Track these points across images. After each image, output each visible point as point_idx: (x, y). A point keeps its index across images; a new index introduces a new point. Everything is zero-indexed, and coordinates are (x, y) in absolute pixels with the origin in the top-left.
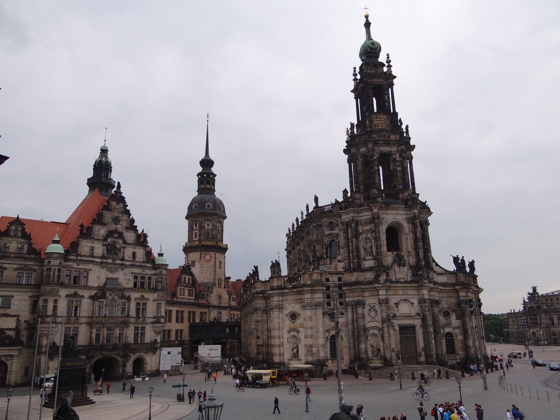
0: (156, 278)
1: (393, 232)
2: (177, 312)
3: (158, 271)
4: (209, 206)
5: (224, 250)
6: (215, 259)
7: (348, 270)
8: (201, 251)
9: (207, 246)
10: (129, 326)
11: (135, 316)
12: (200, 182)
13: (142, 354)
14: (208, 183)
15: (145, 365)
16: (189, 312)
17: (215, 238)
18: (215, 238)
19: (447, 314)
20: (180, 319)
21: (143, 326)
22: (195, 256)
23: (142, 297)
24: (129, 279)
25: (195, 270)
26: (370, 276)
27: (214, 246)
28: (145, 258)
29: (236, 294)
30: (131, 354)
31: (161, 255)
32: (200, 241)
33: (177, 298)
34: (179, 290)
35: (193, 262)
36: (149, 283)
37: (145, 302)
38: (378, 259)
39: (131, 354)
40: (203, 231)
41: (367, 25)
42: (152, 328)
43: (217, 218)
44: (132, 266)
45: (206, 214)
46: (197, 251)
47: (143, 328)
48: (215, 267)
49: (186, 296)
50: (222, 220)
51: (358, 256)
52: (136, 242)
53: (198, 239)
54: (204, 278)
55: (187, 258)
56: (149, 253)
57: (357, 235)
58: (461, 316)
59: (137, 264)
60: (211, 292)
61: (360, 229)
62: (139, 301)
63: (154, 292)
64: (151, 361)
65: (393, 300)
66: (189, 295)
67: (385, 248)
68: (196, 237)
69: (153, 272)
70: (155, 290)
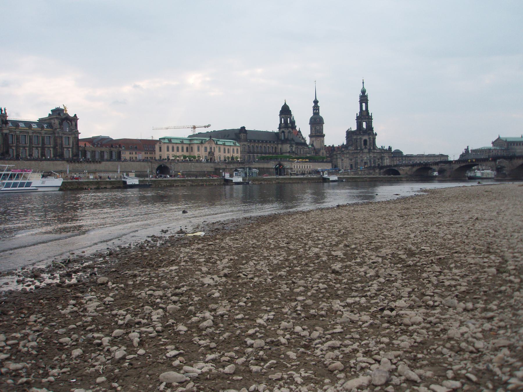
1: (365, 141)
7: (355, 150)
12: (314, 110)
19: (379, 159)
22: (314, 139)
25: (315, 144)
26: (359, 151)
35: (313, 141)
38: (361, 147)
41: (363, 83)
45: (317, 122)
51: (357, 147)
55: (311, 140)
57: (357, 142)
58: (382, 160)
61: (358, 140)
65: (363, 156)
67: (363, 145)
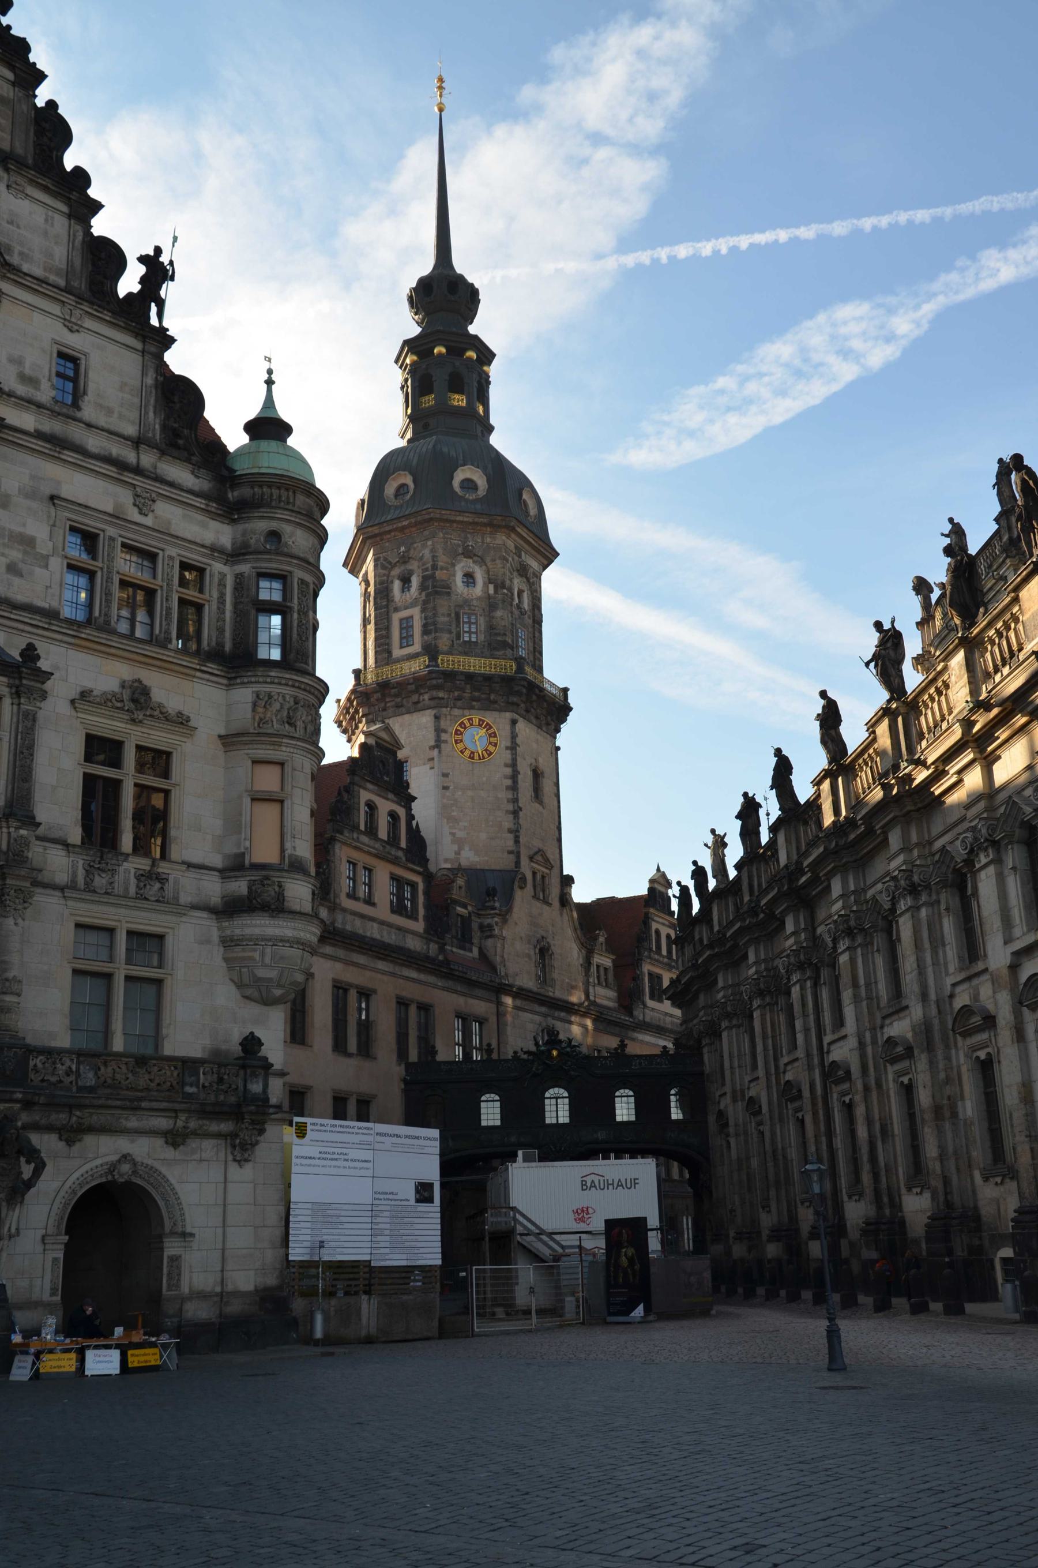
0: (239, 578)
2: (340, 989)
3: (259, 526)
4: (469, 485)
5: (554, 709)
6: (513, 747)
8: (437, 704)
9: (470, 677)
10: (26, 898)
11: (75, 835)
13: (145, 1150)
14: (456, 385)
15: (171, 1248)
16: (402, 1003)
17: (505, 645)
18: (505, 645)
20: (353, 1038)
21: (147, 921)
23: (138, 699)
24: (28, 542)
27: (507, 681)
28: (155, 422)
29: (611, 947)
30: (45, 1143)
31: (268, 427)
32: (431, 651)
33: (334, 907)
34: (344, 870)
36: (191, 607)
37: (158, 737)
39: (45, 1143)
40: (443, 606)
42: (217, 953)
43: (510, 544)
44: (57, 445)
46: (417, 707)
47: (148, 943)
48: (514, 788)
49: (383, 910)
50: (534, 565)
52: (80, 284)
53: (417, 648)
54: (460, 842)
56: (182, 399)
59: (94, 443)
60: (504, 916)
62: (111, 726)
63: (231, 682)
64: (217, 1224)
66: (398, 908)
68: (406, 639)
69: (222, 534)
70: (237, 660)
